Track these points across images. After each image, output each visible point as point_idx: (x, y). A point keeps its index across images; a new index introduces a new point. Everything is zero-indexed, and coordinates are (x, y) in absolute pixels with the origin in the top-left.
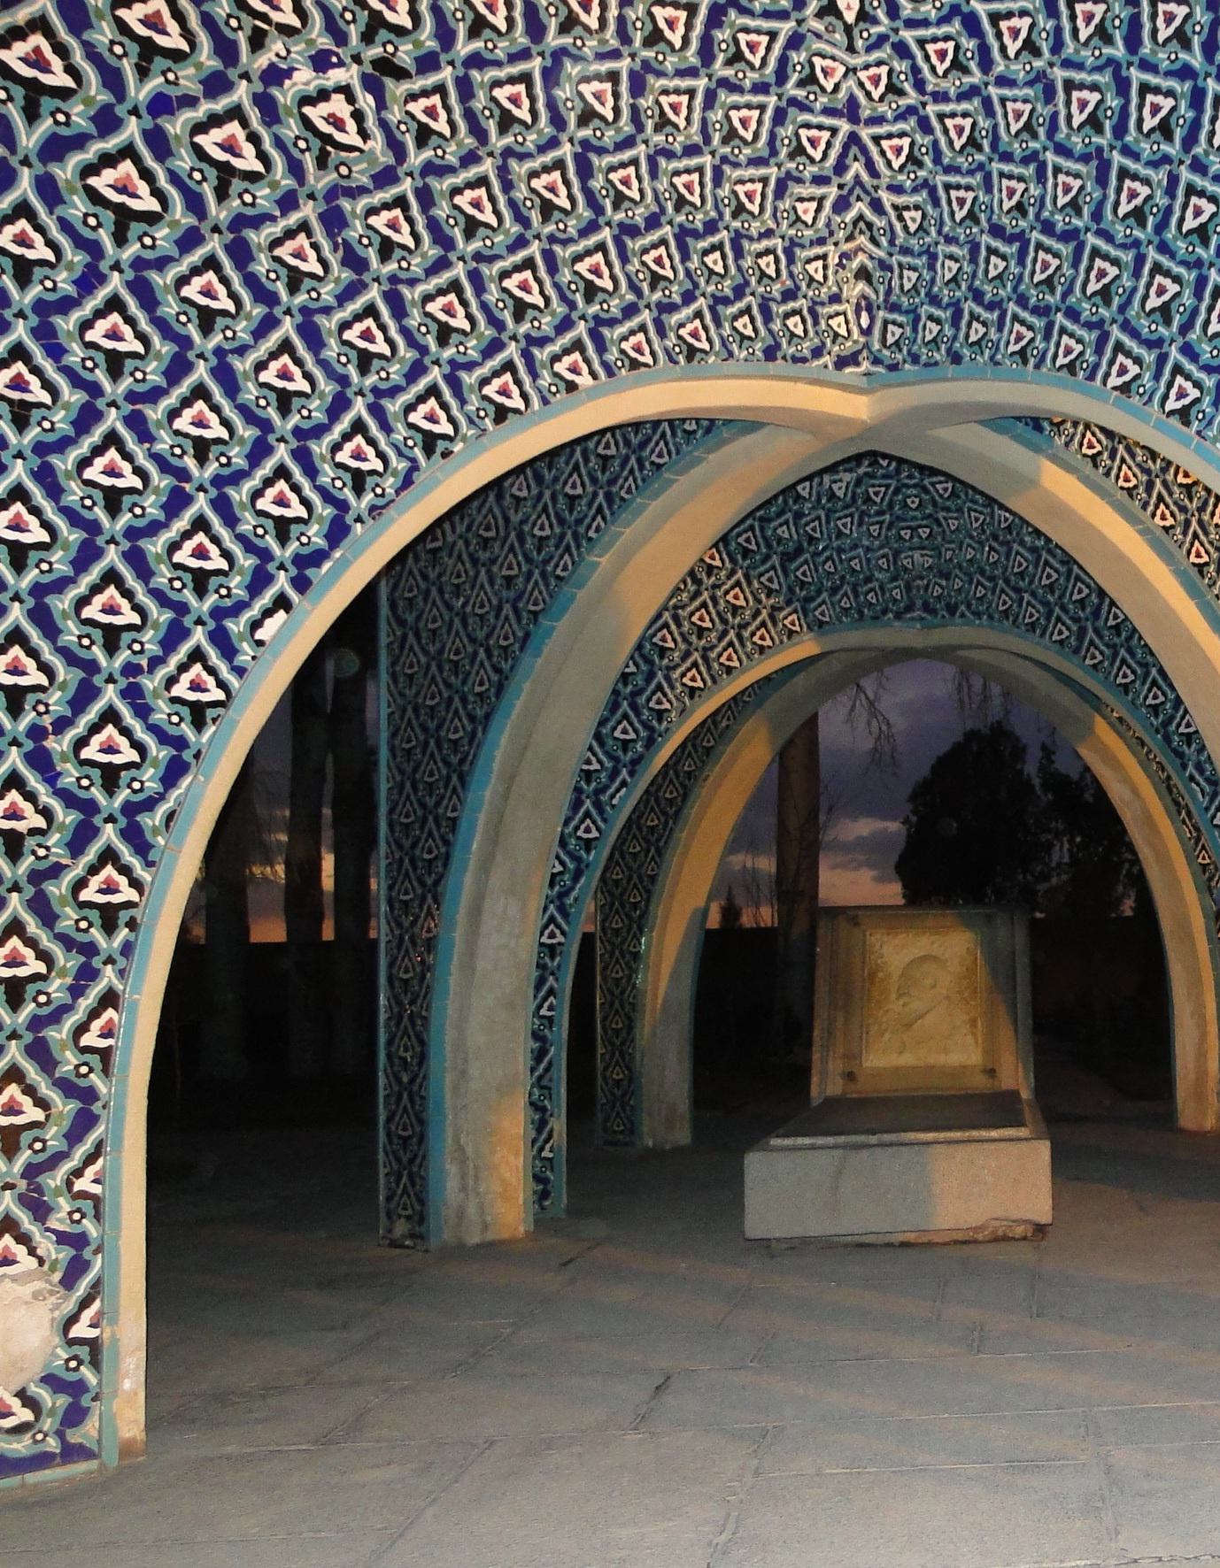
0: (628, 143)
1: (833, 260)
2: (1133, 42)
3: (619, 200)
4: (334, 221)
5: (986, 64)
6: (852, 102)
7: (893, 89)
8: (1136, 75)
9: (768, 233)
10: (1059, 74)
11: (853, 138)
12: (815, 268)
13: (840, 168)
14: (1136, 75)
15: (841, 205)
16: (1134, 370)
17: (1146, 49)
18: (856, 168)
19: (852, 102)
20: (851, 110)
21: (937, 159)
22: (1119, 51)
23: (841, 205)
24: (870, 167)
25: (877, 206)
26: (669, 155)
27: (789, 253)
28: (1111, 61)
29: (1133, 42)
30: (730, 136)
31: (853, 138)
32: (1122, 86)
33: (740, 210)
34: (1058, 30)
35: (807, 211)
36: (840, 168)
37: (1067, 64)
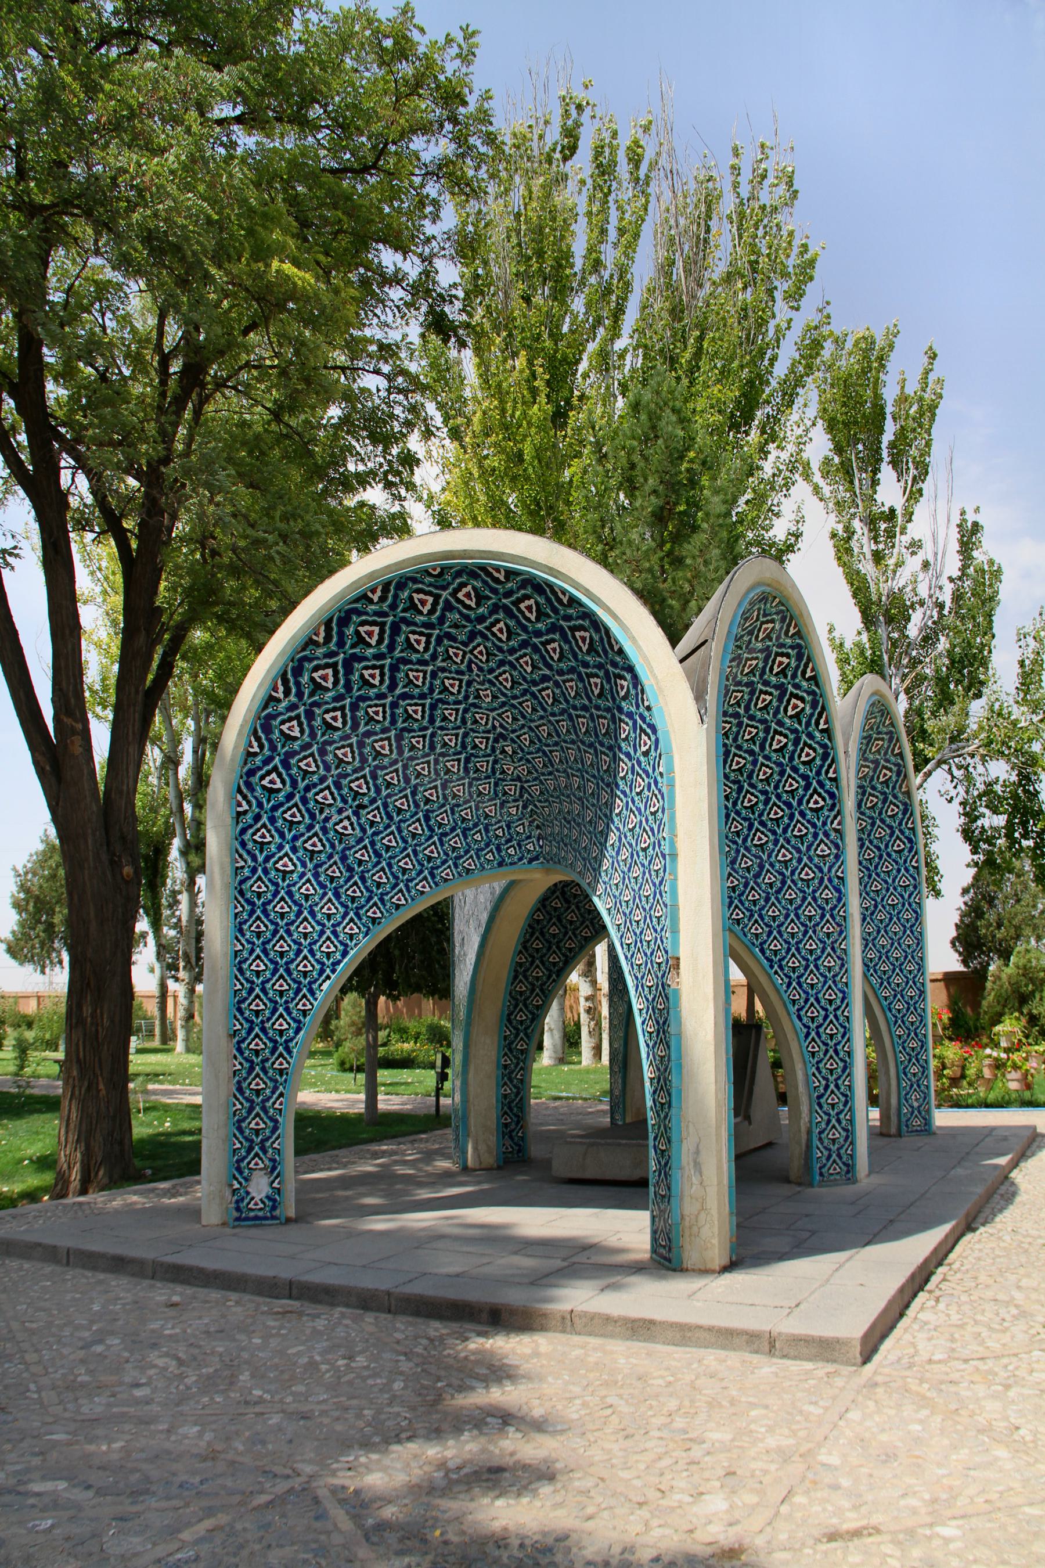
0: (444, 805)
1: (527, 824)
3: (440, 825)
4: (344, 858)
7: (529, 772)
9: (499, 821)
12: (520, 829)
13: (521, 796)
15: (525, 807)
23: (525, 807)
26: (458, 806)
27: (509, 827)
30: (480, 794)
31: (522, 787)
33: (487, 816)
35: (513, 811)
36: (521, 796)
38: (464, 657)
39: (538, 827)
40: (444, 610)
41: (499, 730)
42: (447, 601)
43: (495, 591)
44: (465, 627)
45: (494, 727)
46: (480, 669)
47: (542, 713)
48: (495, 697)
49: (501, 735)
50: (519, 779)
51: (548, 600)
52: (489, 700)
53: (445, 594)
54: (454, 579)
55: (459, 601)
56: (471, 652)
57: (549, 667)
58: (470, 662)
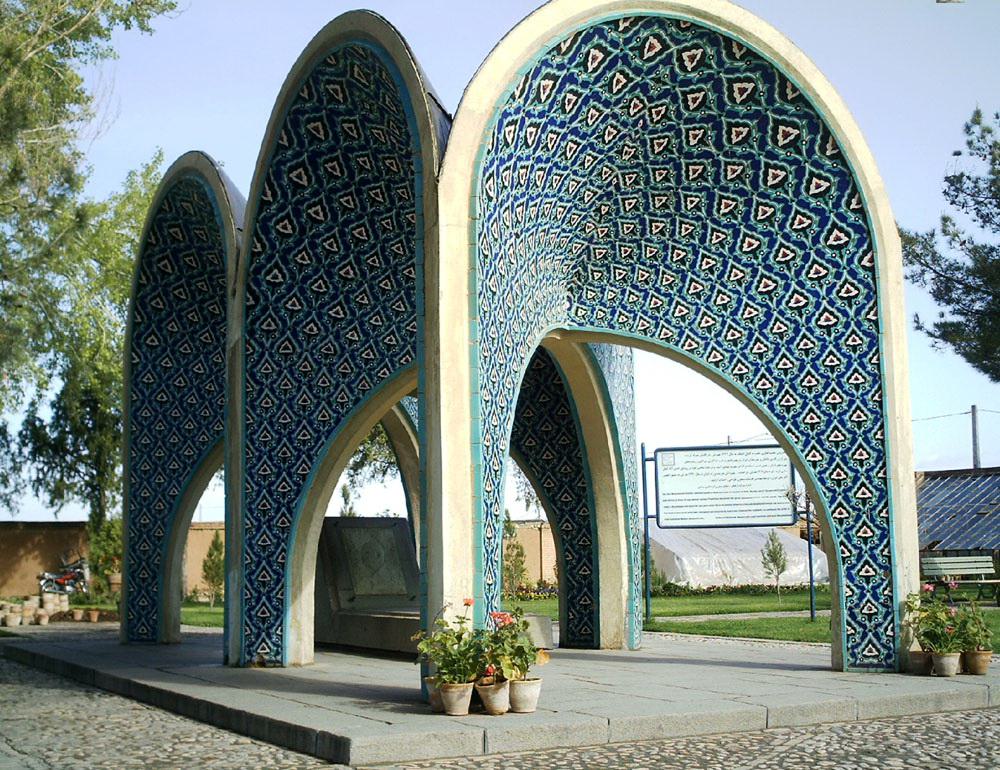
2: (703, 240)
5: (643, 233)
6: (592, 237)
8: (702, 251)
10: (670, 243)
11: (588, 247)
14: (702, 251)
16: (695, 345)
17: (707, 244)
18: (584, 256)
19: (592, 237)
20: (590, 240)
21: (613, 259)
22: (697, 242)
24: (589, 259)
25: (585, 269)
28: (692, 244)
29: (703, 240)
31: (588, 247)
32: (696, 253)
34: (674, 230)
37: (675, 241)
38: (640, 111)
39: (571, 290)
40: (661, 62)
41: (611, 188)
42: (672, 53)
43: (720, 63)
44: (665, 84)
45: (610, 184)
46: (645, 127)
47: (673, 184)
48: (635, 157)
49: (609, 195)
50: (590, 240)
51: (771, 91)
52: (627, 157)
53: (674, 48)
54: (692, 38)
55: (680, 60)
56: (650, 110)
57: (719, 145)
58: (643, 117)
